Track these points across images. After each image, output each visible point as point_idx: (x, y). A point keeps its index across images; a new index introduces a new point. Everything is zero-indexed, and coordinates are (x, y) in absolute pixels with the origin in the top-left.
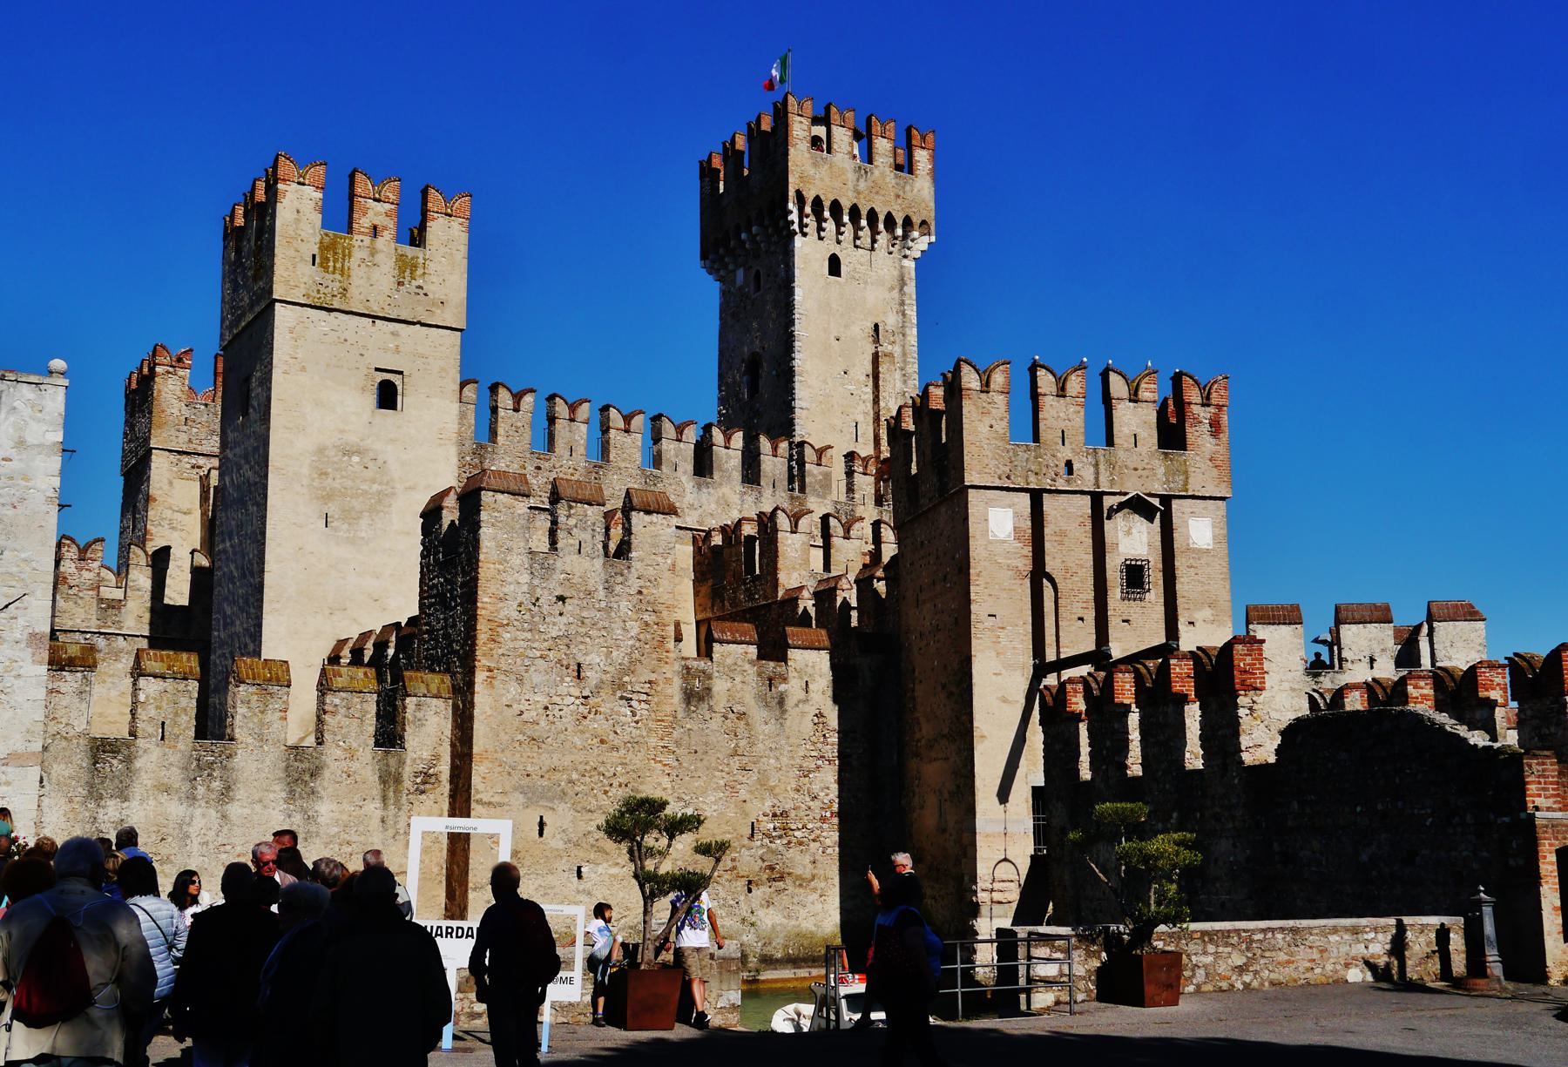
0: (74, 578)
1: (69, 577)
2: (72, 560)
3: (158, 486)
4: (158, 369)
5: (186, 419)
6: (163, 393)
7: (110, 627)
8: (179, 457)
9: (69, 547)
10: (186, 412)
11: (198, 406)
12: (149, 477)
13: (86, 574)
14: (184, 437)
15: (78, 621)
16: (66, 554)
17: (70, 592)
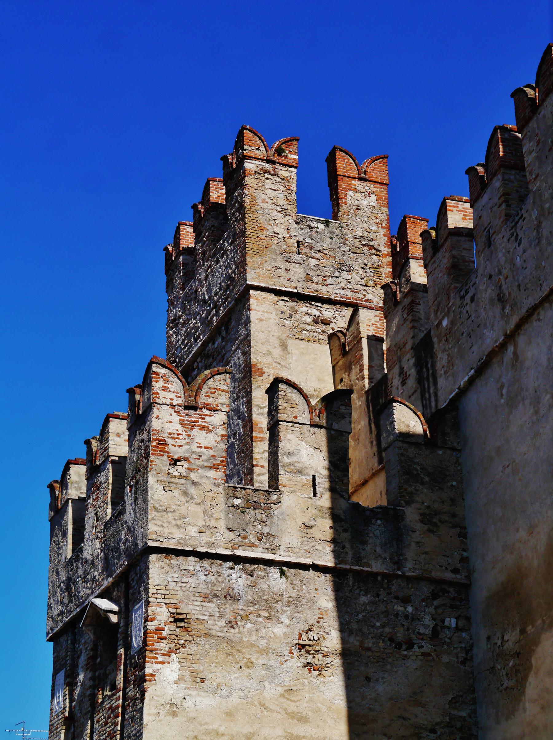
0: (179, 442)
1: (170, 441)
2: (172, 406)
3: (264, 349)
4: (249, 165)
5: (298, 242)
6: (259, 201)
7: (253, 545)
8: (291, 304)
9: (166, 381)
10: (298, 233)
11: (314, 224)
12: (248, 335)
13: (200, 437)
14: (297, 272)
15: (193, 531)
16: (162, 394)
17: (172, 471)
